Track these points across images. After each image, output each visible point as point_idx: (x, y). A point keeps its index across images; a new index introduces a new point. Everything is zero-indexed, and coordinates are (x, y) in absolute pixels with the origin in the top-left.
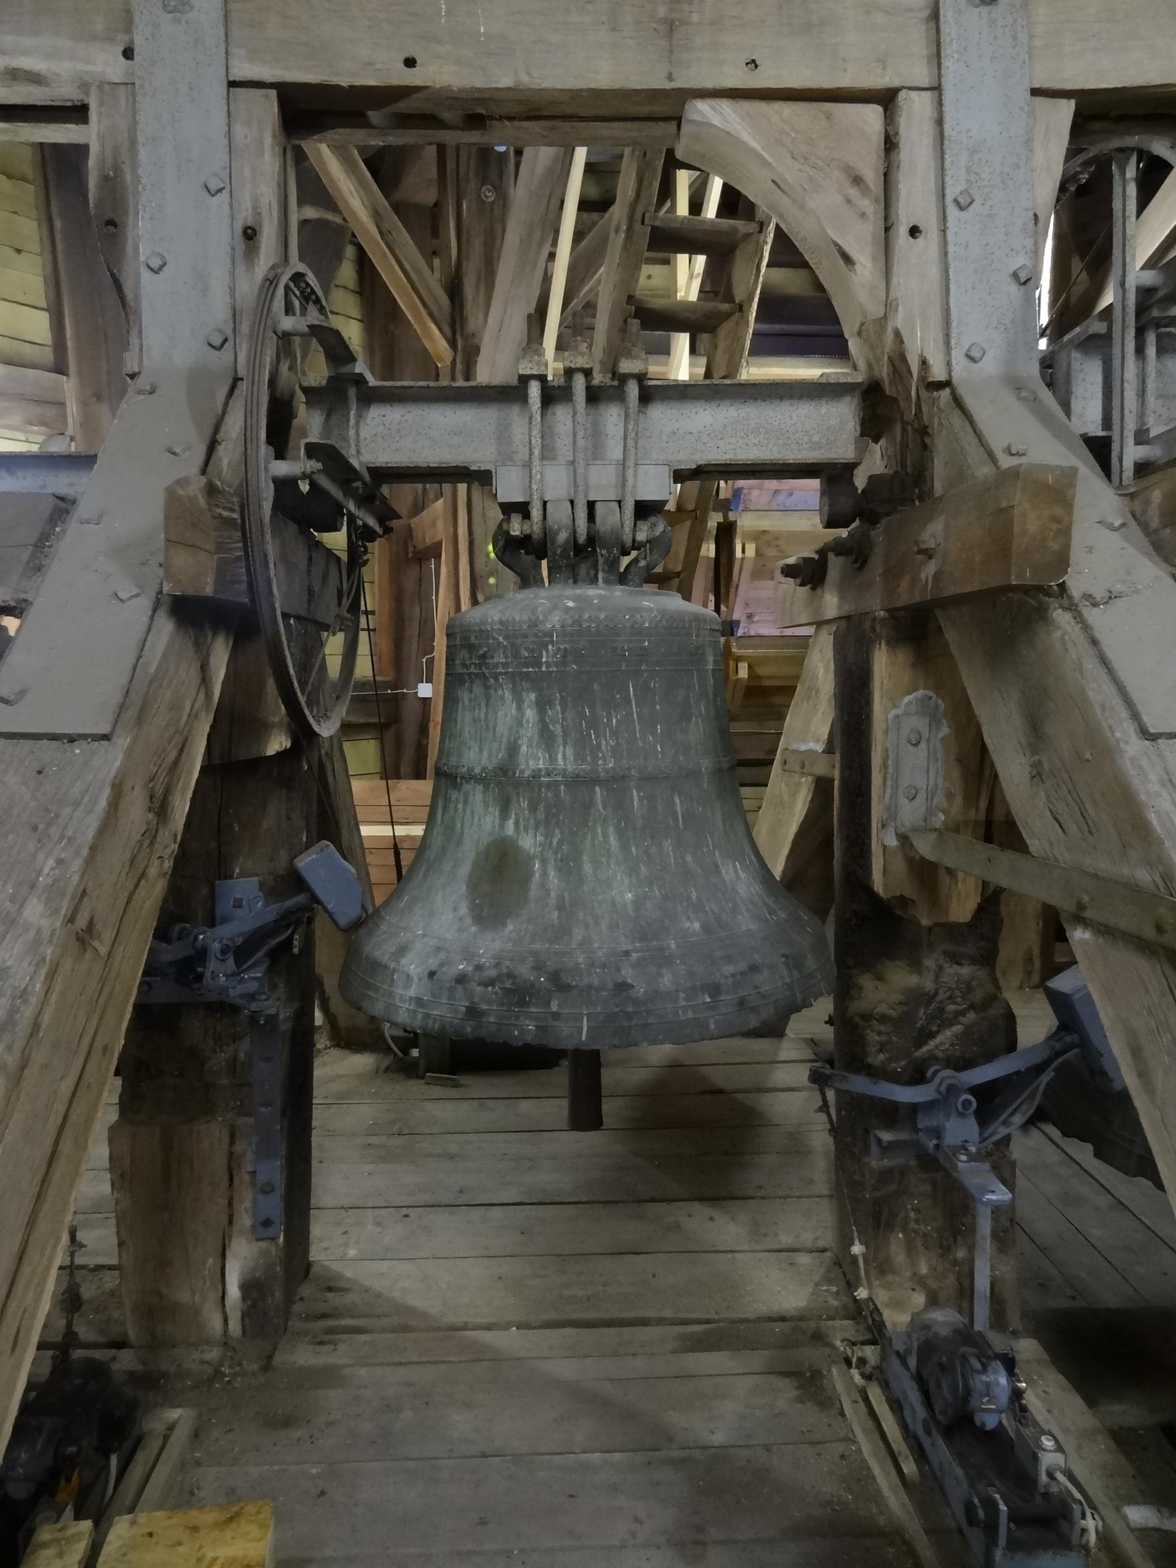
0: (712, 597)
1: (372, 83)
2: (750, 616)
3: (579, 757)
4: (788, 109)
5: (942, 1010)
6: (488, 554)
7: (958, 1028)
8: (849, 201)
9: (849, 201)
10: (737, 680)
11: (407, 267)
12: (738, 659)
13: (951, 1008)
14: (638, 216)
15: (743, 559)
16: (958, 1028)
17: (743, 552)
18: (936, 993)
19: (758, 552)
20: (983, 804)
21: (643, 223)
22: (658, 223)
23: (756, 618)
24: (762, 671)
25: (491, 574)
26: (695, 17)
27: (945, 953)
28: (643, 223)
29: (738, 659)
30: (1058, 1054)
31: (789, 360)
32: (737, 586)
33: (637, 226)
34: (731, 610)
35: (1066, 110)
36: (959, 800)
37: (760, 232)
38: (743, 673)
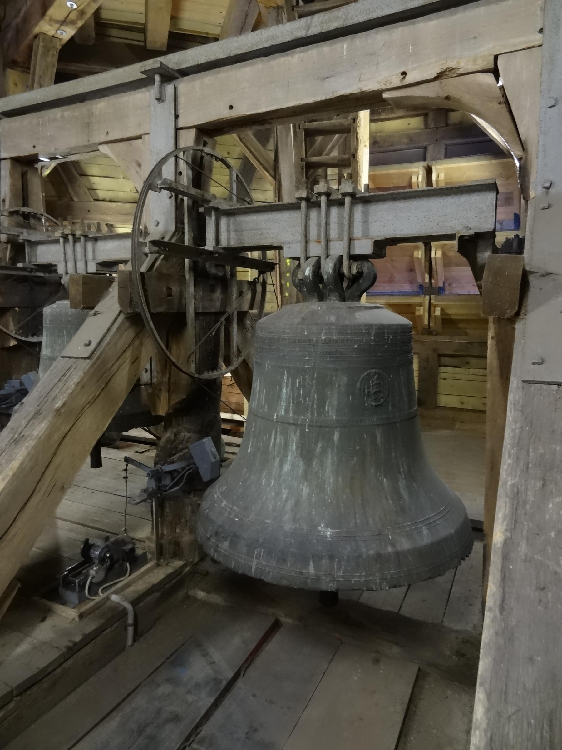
0: (427, 276)
1: (27, 154)
2: (450, 284)
3: (51, 352)
4: (121, 144)
5: (176, 447)
6: (286, 264)
7: (181, 454)
8: (137, 172)
9: (137, 172)
10: (435, 316)
11: (252, 150)
12: (436, 306)
13: (181, 446)
14: (297, 126)
15: (435, 258)
16: (181, 454)
17: (436, 254)
18: (175, 440)
19: (444, 254)
20: (167, 376)
21: (300, 128)
22: (306, 128)
23: (454, 285)
24: (449, 312)
25: (288, 272)
26: (94, 121)
27: (185, 428)
28: (300, 128)
29: (436, 306)
30: (189, 466)
31: (465, 159)
32: (436, 271)
33: (298, 130)
34: (437, 281)
35: (194, 131)
36: (160, 374)
37: (354, 122)
38: (438, 312)
